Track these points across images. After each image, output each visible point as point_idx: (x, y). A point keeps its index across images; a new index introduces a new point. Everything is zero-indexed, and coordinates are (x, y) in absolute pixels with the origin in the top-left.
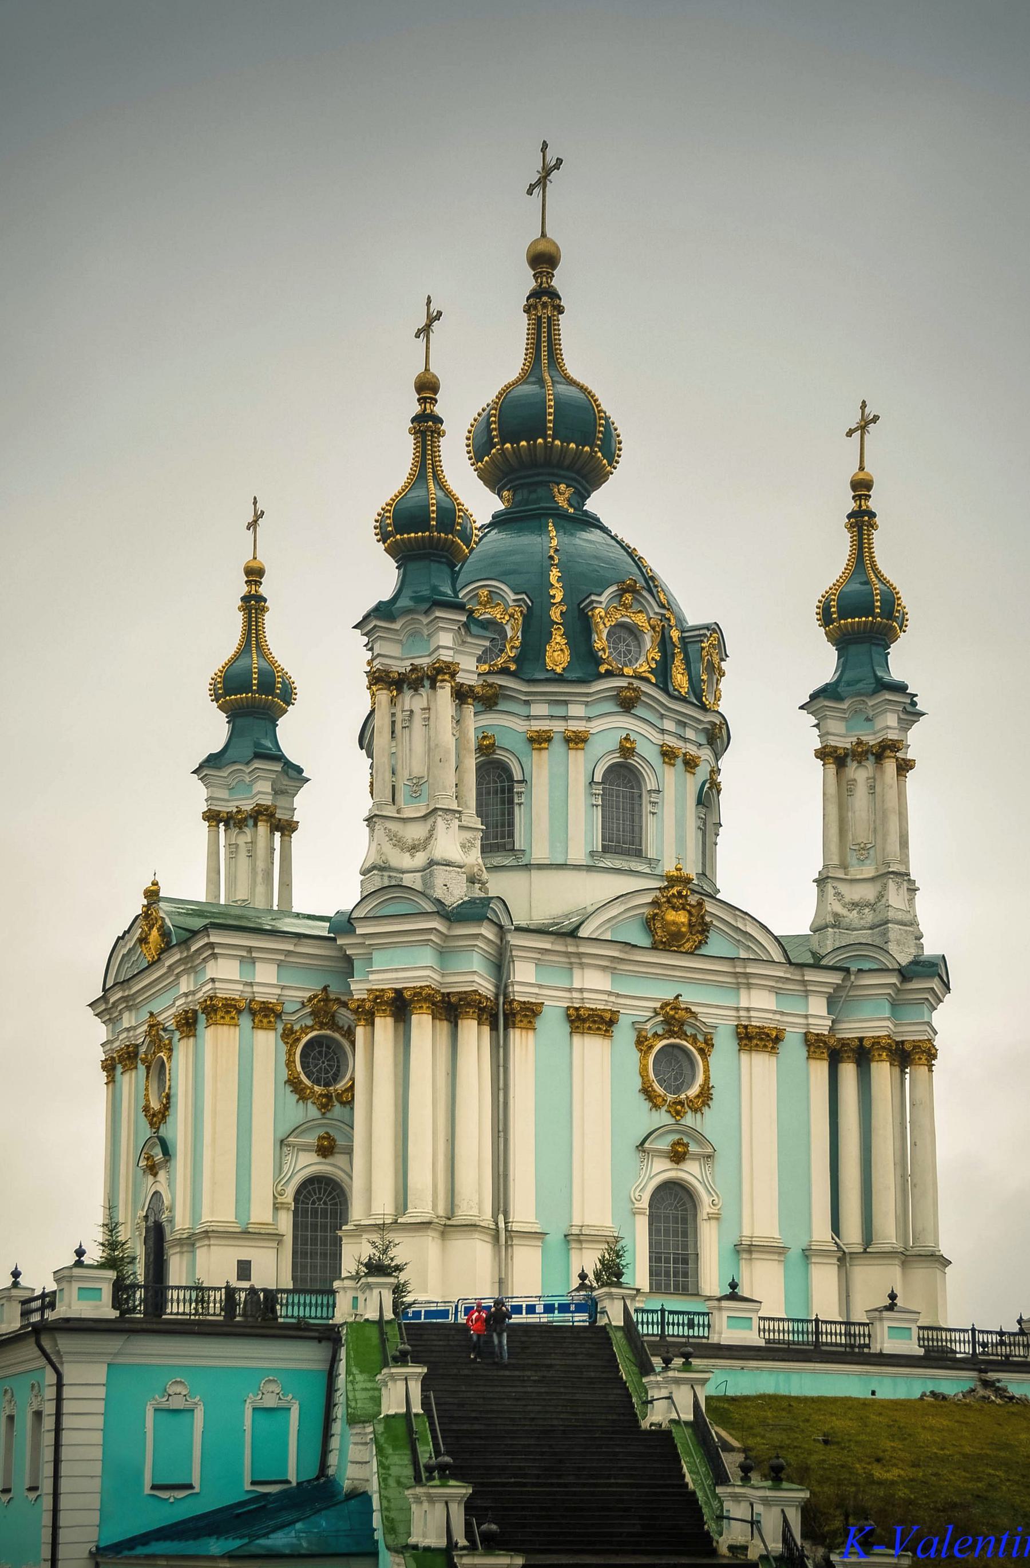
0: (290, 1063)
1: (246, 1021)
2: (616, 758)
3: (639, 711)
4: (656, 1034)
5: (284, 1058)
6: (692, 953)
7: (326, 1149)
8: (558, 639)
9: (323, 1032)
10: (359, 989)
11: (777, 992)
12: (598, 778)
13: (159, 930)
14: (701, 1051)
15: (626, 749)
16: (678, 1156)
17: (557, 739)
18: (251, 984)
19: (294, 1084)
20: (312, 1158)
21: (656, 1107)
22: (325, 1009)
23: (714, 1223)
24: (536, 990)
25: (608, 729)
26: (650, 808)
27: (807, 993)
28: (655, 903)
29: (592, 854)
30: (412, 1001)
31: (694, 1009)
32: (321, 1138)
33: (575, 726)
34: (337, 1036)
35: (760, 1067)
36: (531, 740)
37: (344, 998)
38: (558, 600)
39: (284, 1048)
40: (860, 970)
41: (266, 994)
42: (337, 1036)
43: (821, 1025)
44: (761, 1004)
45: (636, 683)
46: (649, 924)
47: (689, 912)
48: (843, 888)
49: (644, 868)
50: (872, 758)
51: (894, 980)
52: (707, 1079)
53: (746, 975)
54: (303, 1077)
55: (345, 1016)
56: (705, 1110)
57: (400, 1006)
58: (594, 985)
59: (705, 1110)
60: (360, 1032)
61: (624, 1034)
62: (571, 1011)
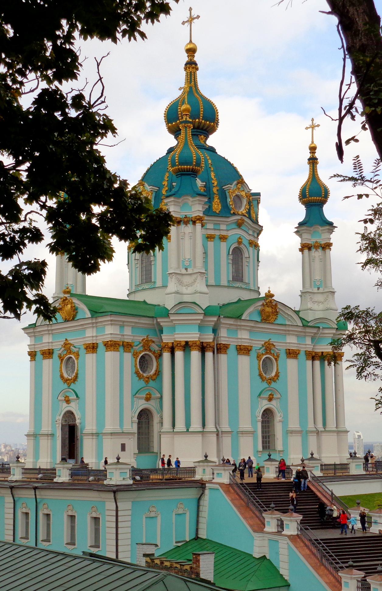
0: (136, 366)
1: (121, 349)
2: (236, 245)
3: (242, 228)
4: (263, 354)
5: (134, 364)
6: (272, 323)
7: (148, 399)
8: (216, 200)
9: (146, 353)
10: (167, 338)
11: (297, 336)
12: (230, 253)
13: (71, 307)
14: (276, 359)
15: (240, 243)
16: (270, 399)
17: (217, 237)
18: (123, 335)
19: (137, 373)
20: (143, 401)
21: (263, 380)
22: (146, 344)
23: (281, 423)
24: (227, 339)
25: (234, 233)
26: (246, 264)
27: (305, 336)
28: (263, 305)
29: (229, 281)
30: (192, 346)
31: (274, 344)
32: (147, 394)
33: (224, 233)
34: (150, 354)
35: (292, 364)
36: (208, 238)
37: (154, 340)
38: (215, 184)
39: (134, 359)
40: (323, 328)
41: (127, 339)
42: (150, 354)
43: (310, 348)
44: (292, 341)
45: (244, 218)
46: (261, 312)
47: (272, 308)
48: (312, 296)
49: (244, 286)
50: (321, 248)
51: (334, 331)
52: (277, 370)
53: (289, 331)
54: (140, 370)
55: (155, 347)
56: (277, 381)
57: (187, 347)
58: (244, 337)
59: (277, 381)
60: (166, 356)
61: (253, 354)
62: (238, 347)
